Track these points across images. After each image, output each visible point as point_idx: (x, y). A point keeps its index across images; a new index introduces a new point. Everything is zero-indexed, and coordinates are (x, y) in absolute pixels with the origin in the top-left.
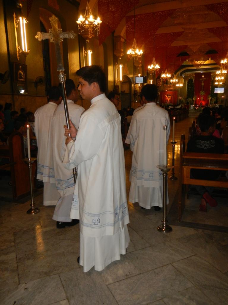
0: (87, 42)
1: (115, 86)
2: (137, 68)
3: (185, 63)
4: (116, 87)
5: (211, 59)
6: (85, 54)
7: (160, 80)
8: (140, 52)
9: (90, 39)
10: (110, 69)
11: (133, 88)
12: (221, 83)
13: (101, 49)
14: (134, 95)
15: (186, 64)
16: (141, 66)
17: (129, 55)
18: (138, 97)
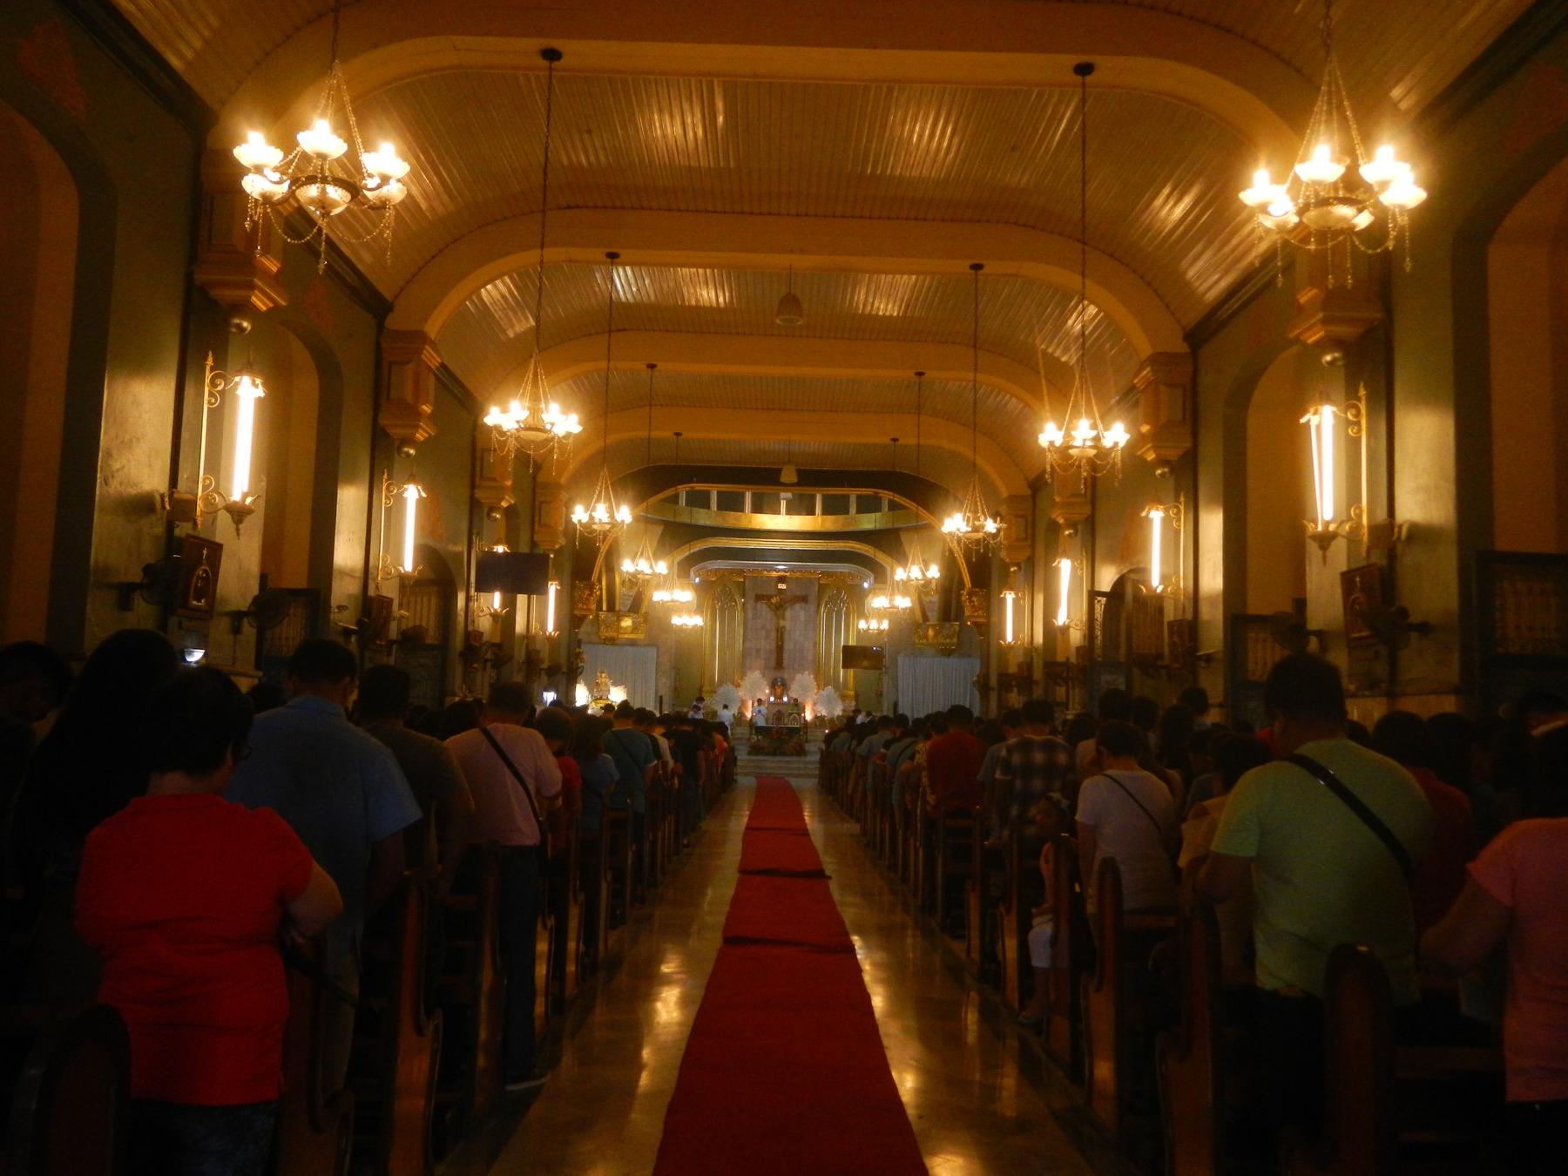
0: (242, 330)
1: (371, 599)
2: (489, 515)
3: (703, 518)
4: (372, 608)
5: (825, 512)
6: (211, 394)
7: (591, 587)
8: (563, 421)
9: (252, 312)
10: (350, 499)
11: (461, 618)
12: (885, 625)
13: (308, 385)
14: (461, 654)
15: (708, 523)
16: (510, 507)
17: (498, 428)
18: (484, 669)
